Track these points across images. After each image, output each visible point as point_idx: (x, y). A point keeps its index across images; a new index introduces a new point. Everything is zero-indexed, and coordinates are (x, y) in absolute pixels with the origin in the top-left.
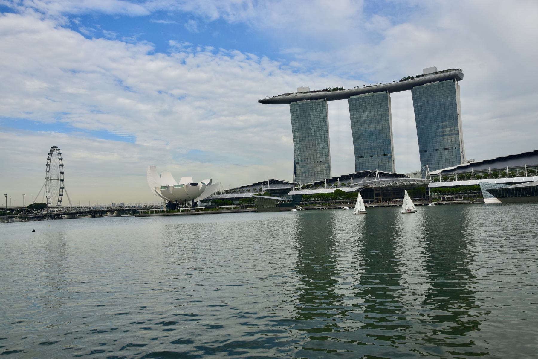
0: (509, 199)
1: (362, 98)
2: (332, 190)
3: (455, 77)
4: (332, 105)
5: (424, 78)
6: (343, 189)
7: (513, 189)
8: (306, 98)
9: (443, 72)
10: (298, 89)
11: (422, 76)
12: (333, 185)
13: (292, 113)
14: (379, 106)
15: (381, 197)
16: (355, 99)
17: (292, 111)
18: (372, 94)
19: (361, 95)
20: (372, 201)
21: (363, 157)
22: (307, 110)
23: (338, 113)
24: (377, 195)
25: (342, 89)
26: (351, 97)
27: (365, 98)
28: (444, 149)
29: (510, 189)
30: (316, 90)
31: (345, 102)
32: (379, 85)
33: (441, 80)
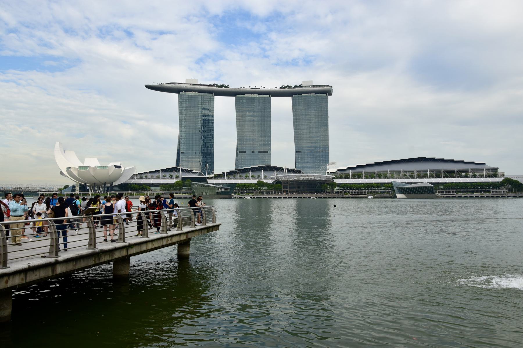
0: (422, 195)
1: (248, 98)
2: (255, 181)
3: (329, 92)
4: (218, 99)
5: (304, 89)
6: (265, 181)
7: (412, 188)
8: (195, 91)
9: (319, 86)
10: (187, 80)
11: (301, 86)
12: (244, 175)
13: (180, 103)
14: (263, 107)
15: (288, 190)
16: (242, 98)
17: (181, 100)
18: (256, 96)
19: (246, 95)
20: (281, 193)
21: (245, 152)
22: (195, 102)
23: (224, 109)
24: (286, 187)
25: (227, 87)
26: (181, 93)
27: (252, 98)
28: (316, 152)
29: (409, 188)
30: (202, 84)
31: (232, 99)
32: (263, 88)
33: (317, 92)
